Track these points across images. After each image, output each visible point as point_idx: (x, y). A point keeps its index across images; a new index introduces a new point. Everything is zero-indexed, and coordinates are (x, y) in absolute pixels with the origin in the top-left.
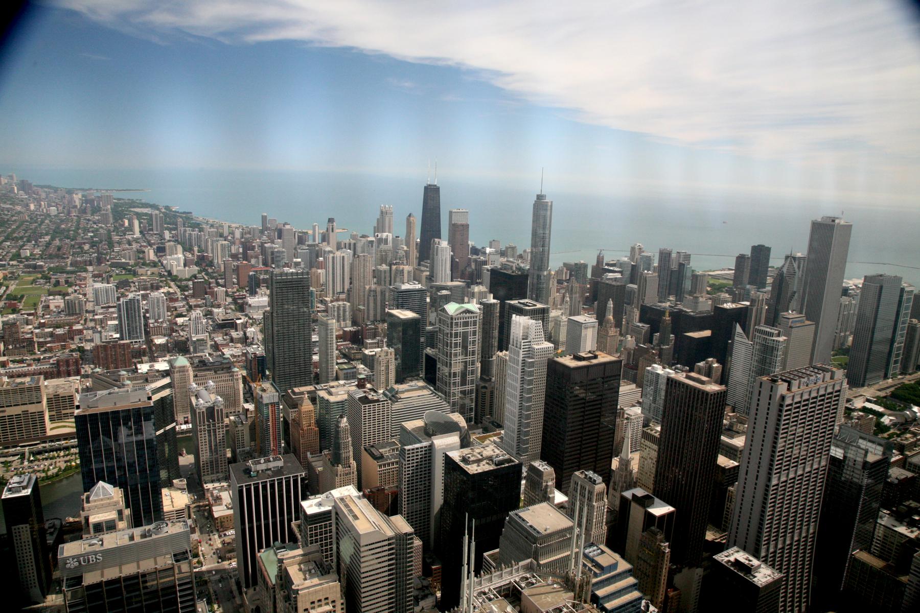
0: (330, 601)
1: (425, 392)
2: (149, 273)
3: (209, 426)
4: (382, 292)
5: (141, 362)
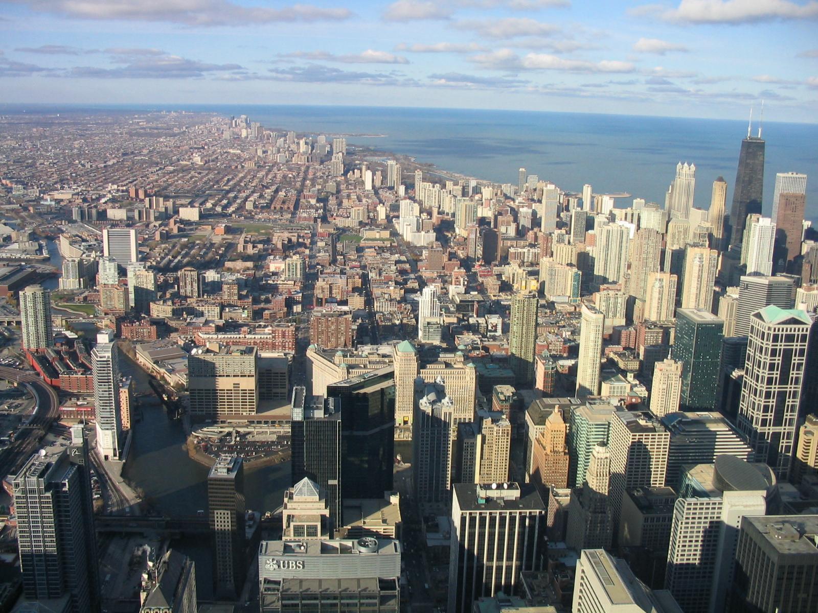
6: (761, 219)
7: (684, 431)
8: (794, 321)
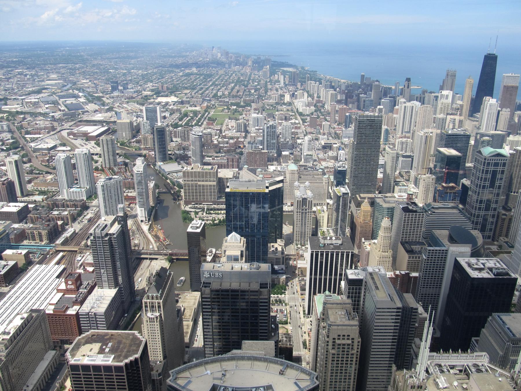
0: (350, 338)
1: (455, 211)
2: (285, 109)
3: (303, 210)
4: (437, 134)
5: (272, 165)
6: (491, 100)
7: (434, 212)
8: (499, 155)
